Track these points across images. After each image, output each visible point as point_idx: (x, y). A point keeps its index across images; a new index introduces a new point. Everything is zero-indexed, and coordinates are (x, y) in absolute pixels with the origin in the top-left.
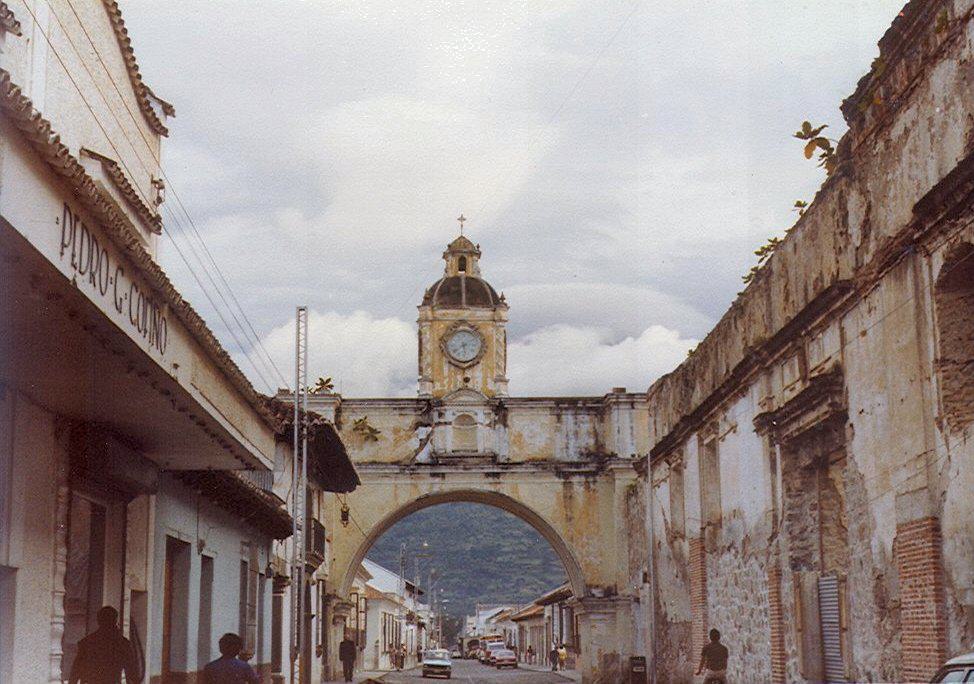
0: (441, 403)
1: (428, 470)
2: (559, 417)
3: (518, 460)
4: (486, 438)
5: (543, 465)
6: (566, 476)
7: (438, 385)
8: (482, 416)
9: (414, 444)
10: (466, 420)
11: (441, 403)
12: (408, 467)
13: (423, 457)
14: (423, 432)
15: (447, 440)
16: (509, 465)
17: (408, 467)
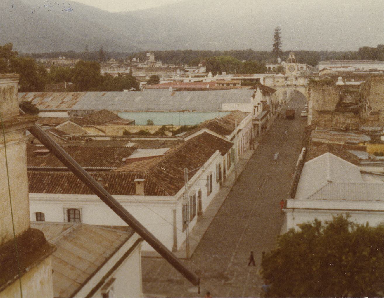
0: (288, 77)
1: (286, 87)
2: (305, 79)
3: (298, 85)
4: (295, 82)
5: (302, 86)
6: (306, 88)
7: (288, 74)
8: (294, 79)
9: (285, 83)
10: (292, 80)
11: (288, 77)
12: (283, 86)
13: (286, 85)
14: (286, 81)
15: (289, 82)
16: (298, 86)
17: (283, 86)
